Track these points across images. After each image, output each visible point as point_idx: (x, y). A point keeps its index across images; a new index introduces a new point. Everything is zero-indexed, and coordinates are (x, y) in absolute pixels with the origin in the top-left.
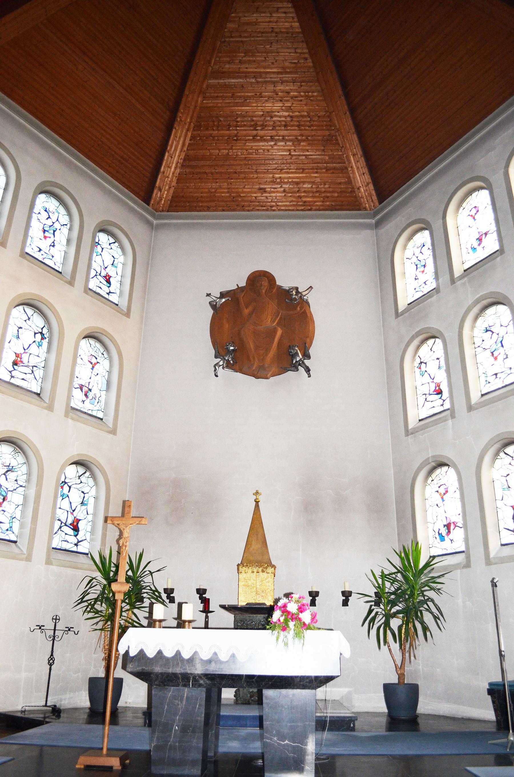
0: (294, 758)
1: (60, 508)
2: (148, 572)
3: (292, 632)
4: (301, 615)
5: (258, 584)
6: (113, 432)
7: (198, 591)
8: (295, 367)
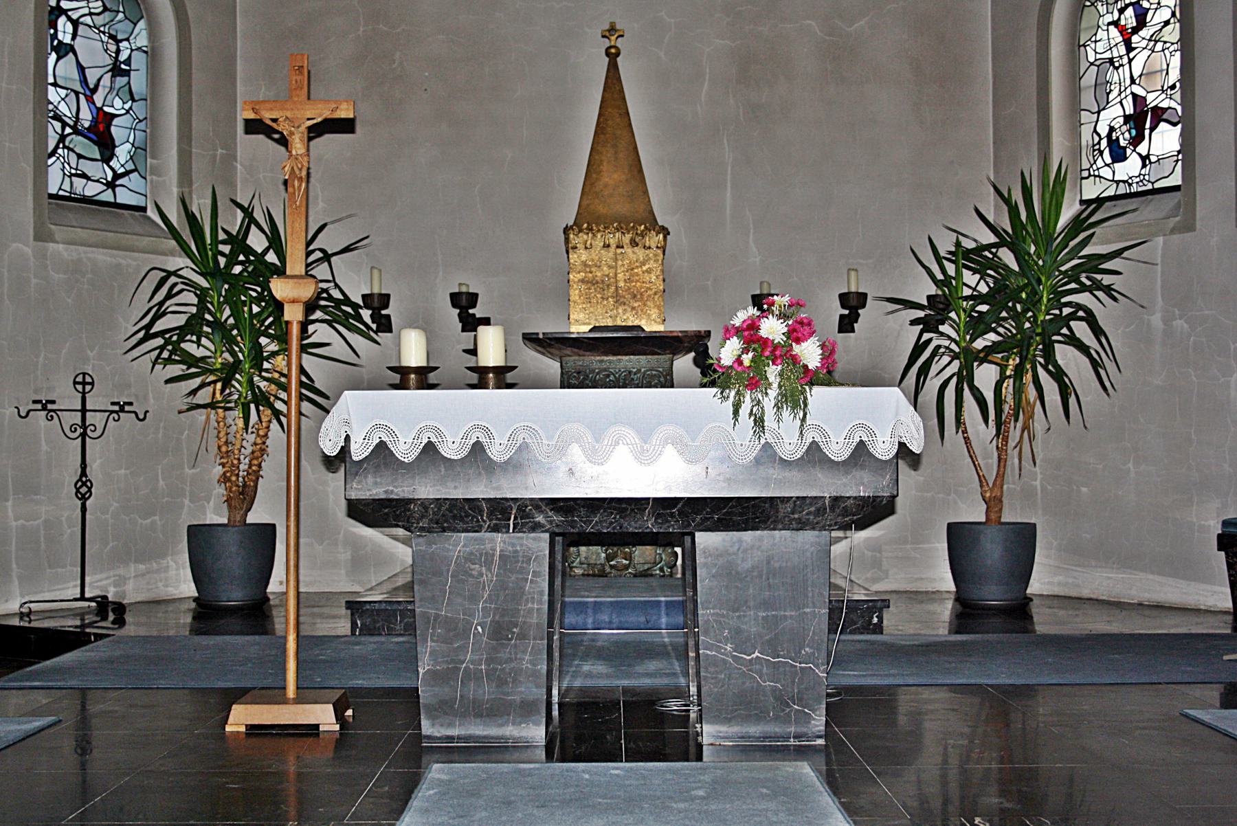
0: (774, 689)
1: (55, 85)
2: (318, 255)
3: (773, 393)
4: (797, 349)
5: (620, 276)
7: (455, 299)
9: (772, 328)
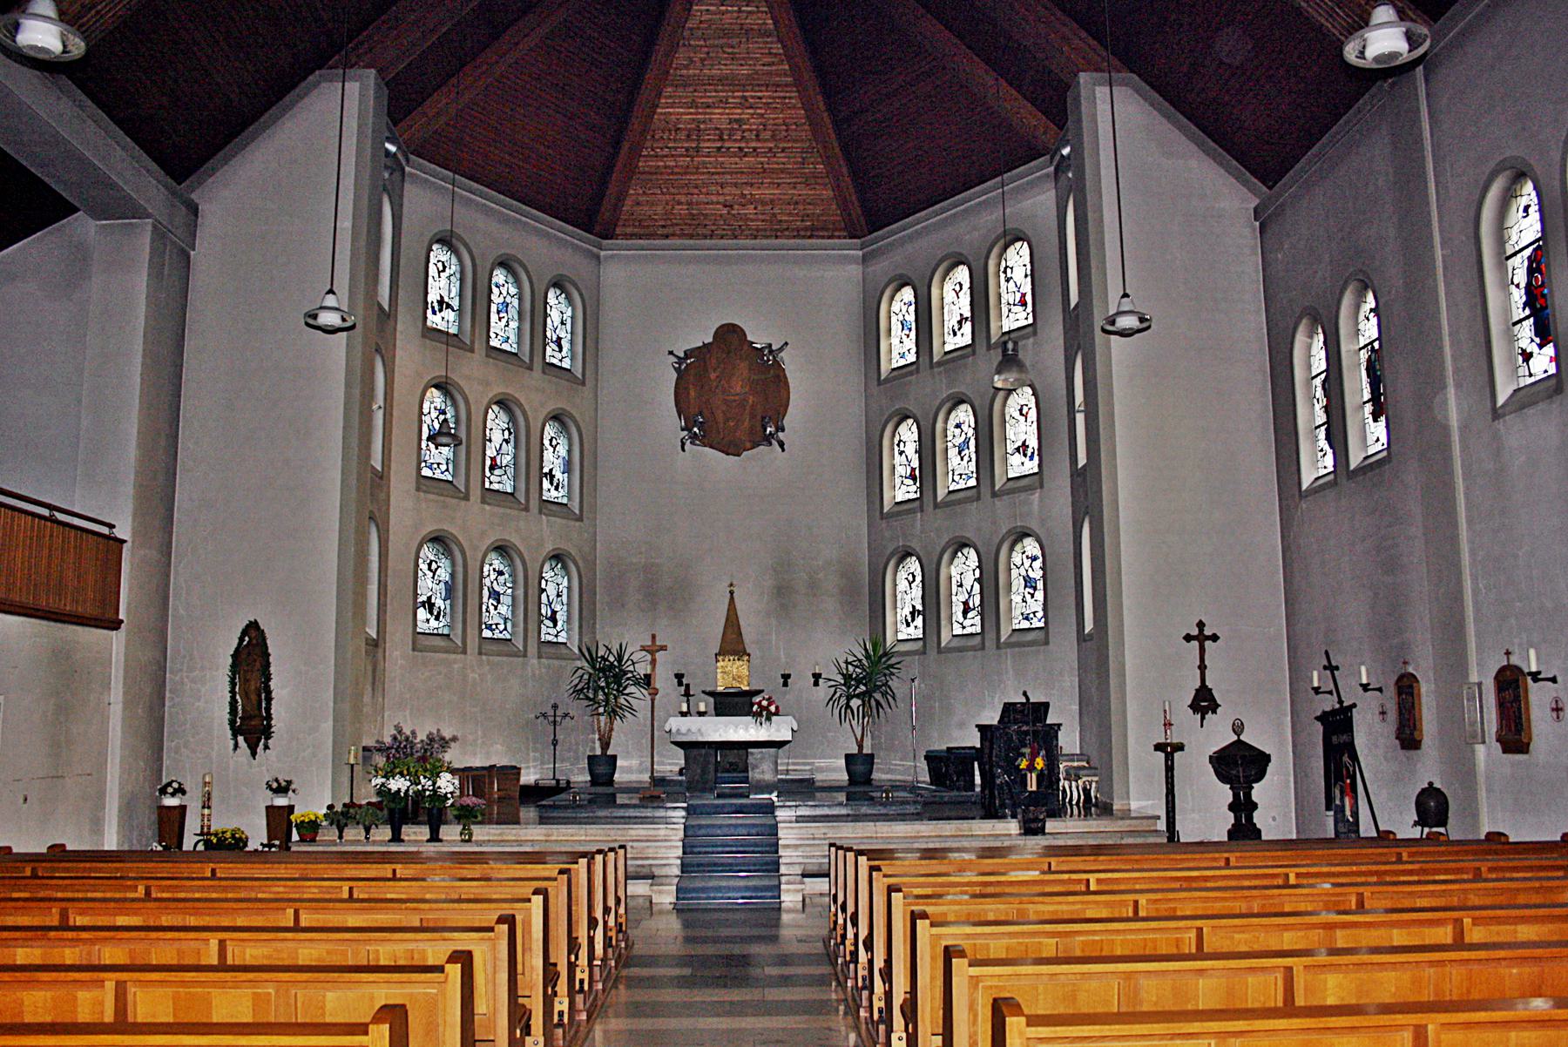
6: (580, 519)
8: (768, 440)
9: (765, 703)
